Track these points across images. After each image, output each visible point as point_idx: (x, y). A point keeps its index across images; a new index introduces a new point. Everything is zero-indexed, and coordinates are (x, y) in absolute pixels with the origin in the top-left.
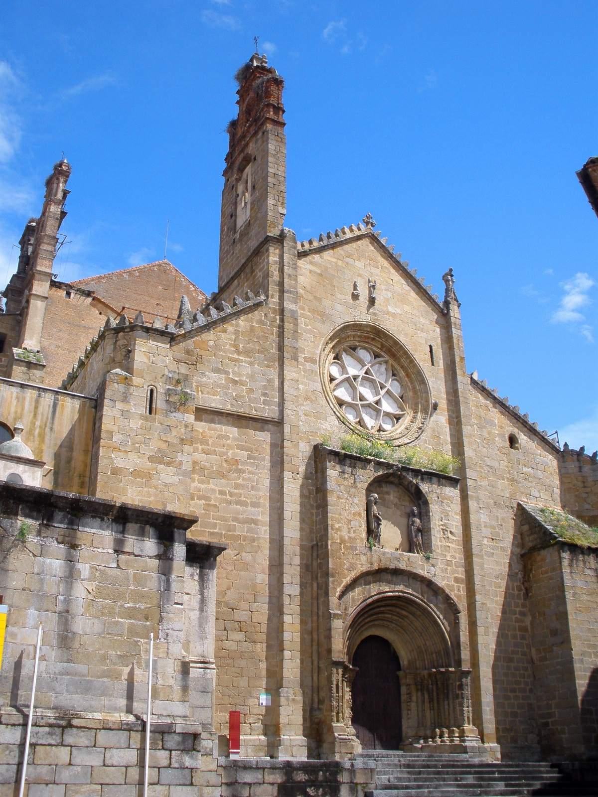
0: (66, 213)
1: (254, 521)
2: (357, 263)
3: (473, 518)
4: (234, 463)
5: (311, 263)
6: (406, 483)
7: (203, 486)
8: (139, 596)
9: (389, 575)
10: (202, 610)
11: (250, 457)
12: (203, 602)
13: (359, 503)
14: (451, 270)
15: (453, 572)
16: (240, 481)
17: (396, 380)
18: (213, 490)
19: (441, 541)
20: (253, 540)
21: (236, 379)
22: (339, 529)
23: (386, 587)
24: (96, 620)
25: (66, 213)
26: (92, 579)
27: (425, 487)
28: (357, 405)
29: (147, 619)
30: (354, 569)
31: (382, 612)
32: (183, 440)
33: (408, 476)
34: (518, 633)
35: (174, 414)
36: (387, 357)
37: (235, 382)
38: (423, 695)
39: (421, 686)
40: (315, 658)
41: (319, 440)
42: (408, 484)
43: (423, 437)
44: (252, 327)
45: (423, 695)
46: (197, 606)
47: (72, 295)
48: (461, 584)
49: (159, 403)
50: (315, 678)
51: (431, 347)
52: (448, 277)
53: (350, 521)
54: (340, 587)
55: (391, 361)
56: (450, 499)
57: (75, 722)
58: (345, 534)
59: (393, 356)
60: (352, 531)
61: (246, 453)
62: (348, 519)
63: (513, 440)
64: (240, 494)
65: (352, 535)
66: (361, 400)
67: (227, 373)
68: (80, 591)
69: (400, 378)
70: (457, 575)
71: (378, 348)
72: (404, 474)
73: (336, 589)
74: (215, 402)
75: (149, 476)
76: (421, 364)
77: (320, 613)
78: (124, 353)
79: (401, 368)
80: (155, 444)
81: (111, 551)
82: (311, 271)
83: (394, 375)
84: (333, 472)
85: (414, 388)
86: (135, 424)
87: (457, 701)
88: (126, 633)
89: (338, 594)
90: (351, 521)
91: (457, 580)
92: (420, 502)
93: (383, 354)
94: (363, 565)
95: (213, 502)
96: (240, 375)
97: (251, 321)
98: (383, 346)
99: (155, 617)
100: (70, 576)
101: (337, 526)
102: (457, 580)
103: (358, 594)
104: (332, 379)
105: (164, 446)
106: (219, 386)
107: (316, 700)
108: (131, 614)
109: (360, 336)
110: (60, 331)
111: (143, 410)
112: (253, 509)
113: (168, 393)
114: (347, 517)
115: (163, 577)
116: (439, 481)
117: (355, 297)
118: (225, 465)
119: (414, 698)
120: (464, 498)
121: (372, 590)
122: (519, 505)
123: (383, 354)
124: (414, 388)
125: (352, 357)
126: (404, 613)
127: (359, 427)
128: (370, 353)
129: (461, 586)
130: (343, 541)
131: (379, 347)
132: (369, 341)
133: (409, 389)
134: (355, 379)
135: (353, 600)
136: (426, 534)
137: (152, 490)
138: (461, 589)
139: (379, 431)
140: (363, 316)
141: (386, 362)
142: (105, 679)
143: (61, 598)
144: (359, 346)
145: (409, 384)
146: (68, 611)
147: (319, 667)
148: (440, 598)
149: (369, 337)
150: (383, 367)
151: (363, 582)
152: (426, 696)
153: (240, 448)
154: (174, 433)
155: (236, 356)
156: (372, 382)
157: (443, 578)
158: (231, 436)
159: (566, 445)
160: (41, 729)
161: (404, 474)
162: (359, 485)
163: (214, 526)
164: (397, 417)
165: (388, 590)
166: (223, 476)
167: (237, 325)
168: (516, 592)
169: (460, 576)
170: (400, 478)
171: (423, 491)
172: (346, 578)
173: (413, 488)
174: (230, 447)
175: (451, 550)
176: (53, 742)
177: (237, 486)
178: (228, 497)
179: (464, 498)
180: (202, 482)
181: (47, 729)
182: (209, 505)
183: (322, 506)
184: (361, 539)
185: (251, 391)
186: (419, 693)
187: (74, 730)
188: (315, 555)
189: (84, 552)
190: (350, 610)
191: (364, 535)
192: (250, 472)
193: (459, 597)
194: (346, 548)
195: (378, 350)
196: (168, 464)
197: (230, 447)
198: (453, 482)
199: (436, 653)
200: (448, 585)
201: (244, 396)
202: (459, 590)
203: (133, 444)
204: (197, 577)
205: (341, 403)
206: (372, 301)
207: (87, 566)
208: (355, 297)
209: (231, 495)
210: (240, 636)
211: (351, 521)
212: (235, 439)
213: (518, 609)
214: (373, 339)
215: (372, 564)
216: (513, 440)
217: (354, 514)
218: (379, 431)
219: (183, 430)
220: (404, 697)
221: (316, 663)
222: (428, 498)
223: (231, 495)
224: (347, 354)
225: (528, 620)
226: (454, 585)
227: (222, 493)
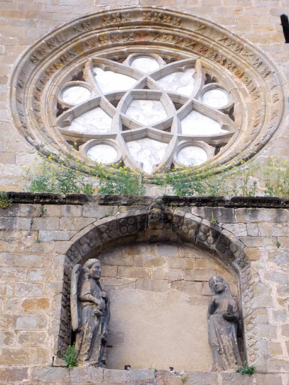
6: (192, 231)
13: (47, 279)
17: (217, 87)
27: (236, 229)
28: (114, 136)
33: (188, 216)
36: (190, 57)
42: (196, 233)
55: (200, 61)
60: (15, 339)
62: (7, 316)
65: (16, 346)
66: (124, 128)
69: (224, 82)
71: (171, 46)
72: (177, 211)
76: (258, 45)
79: (223, 65)
90: (15, 318)
109: (124, 35)
114: (7, 312)
123: (182, 53)
125: (116, 72)
128: (157, 60)
131: (173, 43)
132: (150, 39)
133: (245, 95)
136: (250, 326)
144: (130, 52)
145: (244, 86)
149: (146, 34)
150: (190, 73)
156: (159, 100)
161: (177, 211)
162: (49, 248)
164: (217, 142)
170: (167, 219)
171: (232, 238)
173: (210, 238)
184: (42, 353)
191: (51, 342)
205: (78, 141)
211: (15, 318)
214: (157, 34)
217: (27, 305)
222: (245, 250)
224: (106, 69)
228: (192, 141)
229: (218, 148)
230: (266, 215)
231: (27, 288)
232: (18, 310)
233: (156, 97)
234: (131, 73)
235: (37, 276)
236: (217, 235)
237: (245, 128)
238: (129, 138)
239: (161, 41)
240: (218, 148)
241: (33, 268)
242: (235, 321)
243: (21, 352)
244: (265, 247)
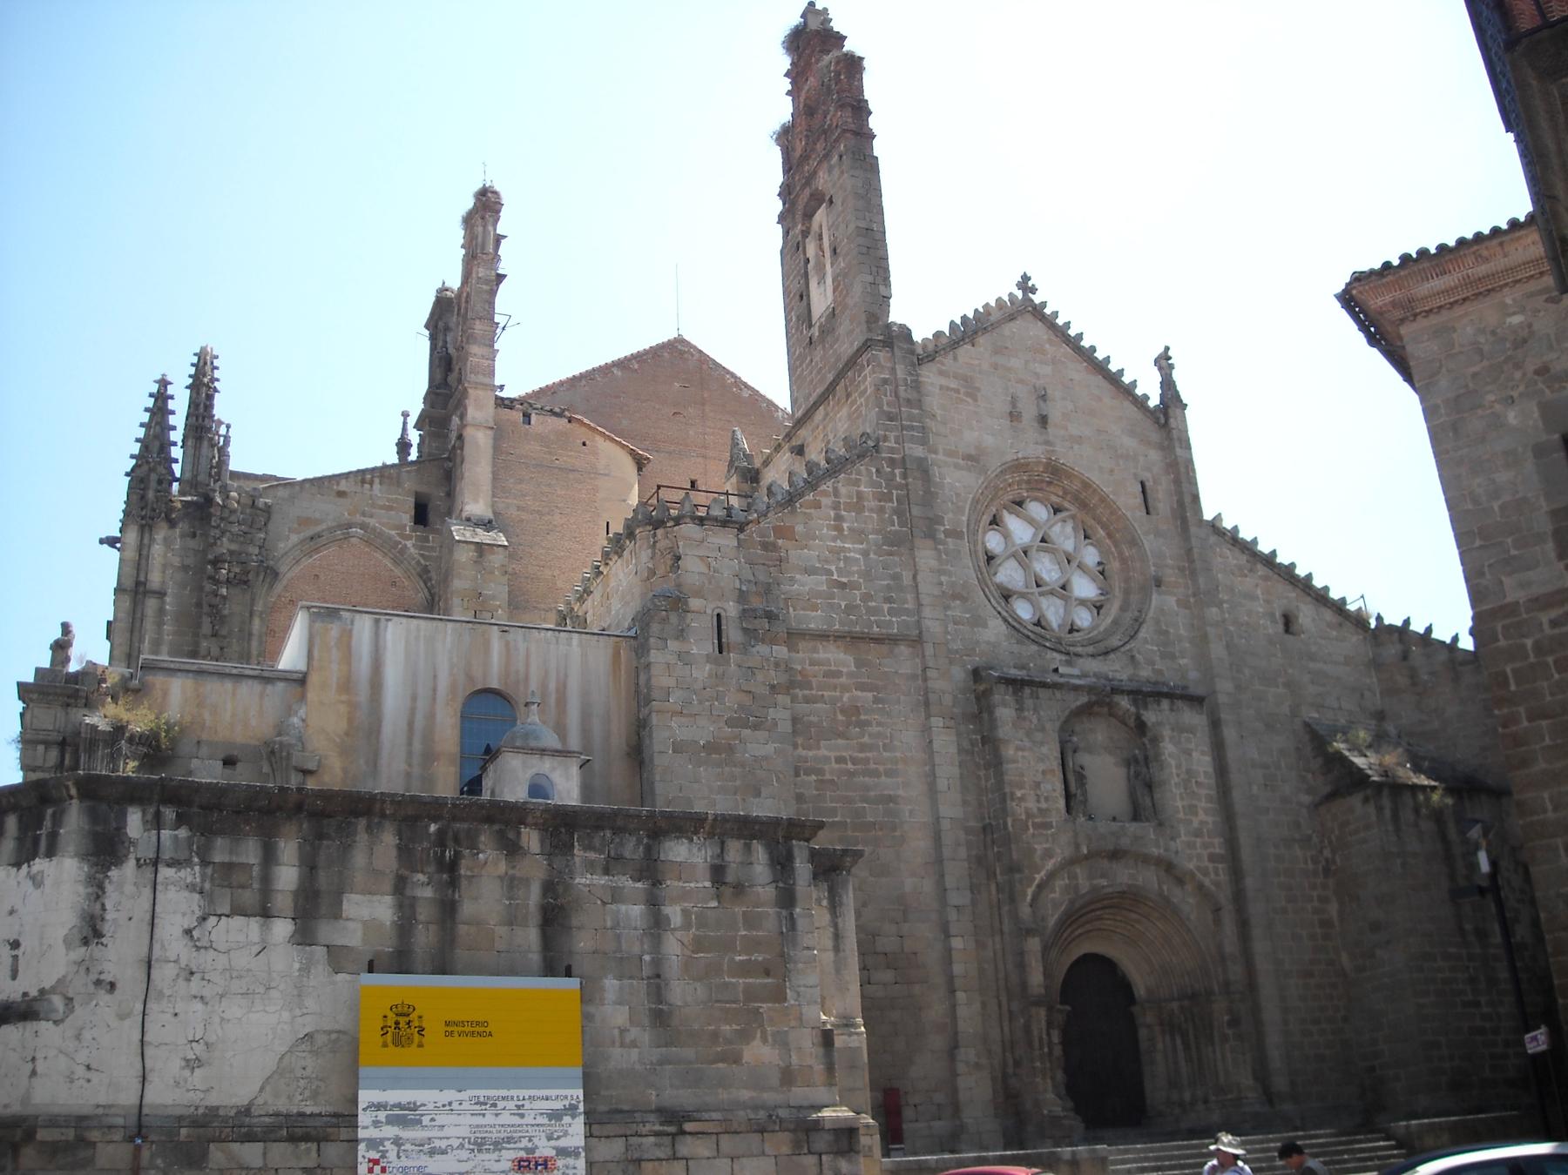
0: (504, 276)
1: (891, 799)
2: (1015, 363)
3: (1232, 754)
4: (853, 711)
5: (941, 373)
7: (811, 754)
8: (752, 945)
10: (837, 949)
11: (876, 700)
12: (837, 937)
13: (1051, 751)
14: (1167, 349)
15: (1205, 846)
16: (866, 739)
18: (827, 759)
19: (1182, 799)
20: (894, 829)
21: (844, 580)
22: (1022, 799)
24: (698, 985)
25: (504, 276)
26: (686, 926)
27: (1150, 717)
29: (767, 973)
30: (1051, 857)
31: (1100, 918)
32: (773, 687)
34: (1319, 931)
35: (757, 648)
36: (1073, 510)
37: (843, 586)
38: (1173, 1040)
40: (1004, 1000)
41: (977, 660)
43: (1142, 634)
44: (860, 496)
45: (1173, 1040)
46: (829, 944)
47: (534, 418)
49: (733, 634)
50: (1006, 1029)
51: (1143, 484)
52: (1164, 362)
53: (1038, 785)
54: (1029, 886)
56: (1191, 730)
57: (688, 1127)
58: (1031, 804)
59: (1083, 505)
61: (870, 695)
63: (1288, 622)
64: (867, 761)
65: (1044, 805)
66: (1038, 586)
67: (830, 573)
68: (673, 947)
74: (815, 620)
75: (730, 749)
76: (1129, 514)
77: (1006, 928)
78: (670, 563)
80: (732, 700)
81: (708, 884)
82: (941, 387)
83: (1086, 537)
84: (1005, 713)
85: (1121, 553)
86: (702, 673)
88: (741, 997)
89: (1029, 898)
91: (1212, 858)
92: (1146, 741)
93: (1066, 504)
94: (1062, 852)
95: (828, 777)
96: (850, 573)
97: (857, 483)
98: (1066, 492)
99: (776, 969)
100: (657, 923)
101: (1019, 794)
102: (1212, 858)
104: (990, 558)
105: (747, 700)
106: (819, 594)
107: (1011, 1062)
108: (745, 969)
109: (1028, 482)
110: (521, 481)
111: (710, 647)
112: (889, 780)
113: (745, 614)
115: (784, 913)
116: (1172, 703)
117: (1014, 416)
118: (840, 717)
119: (1160, 1046)
120: (1215, 725)
122: (1307, 725)
124: (1121, 553)
126: (1134, 916)
127: (1038, 629)
130: (1029, 815)
134: (1025, 553)
137: (737, 770)
139: (1071, 631)
140: (1030, 448)
141: (1073, 517)
142: (721, 1065)
143: (647, 958)
146: (658, 976)
147: (1010, 1012)
148: (1189, 887)
152: (1179, 1041)
153: (862, 687)
154: (760, 677)
155: (839, 543)
158: (845, 670)
159: (1379, 618)
160: (644, 1140)
163: (834, 812)
166: (841, 735)
167: (836, 493)
168: (1311, 866)
169: (1217, 851)
174: (845, 689)
175: (1201, 812)
176: (662, 1156)
177: (863, 748)
178: (850, 766)
179: (1215, 725)
180: (810, 749)
181: (652, 1139)
182: (822, 781)
183: (996, 763)
185: (867, 597)
186: (1168, 1038)
187: (689, 1138)
188: (989, 838)
189: (672, 884)
191: (1062, 803)
192: (879, 724)
193: (1217, 884)
194: (1035, 826)
195: (1058, 500)
196: (756, 727)
197: (845, 689)
198: (1196, 701)
200: (1198, 868)
201: (857, 606)
203: (700, 702)
204: (825, 903)
205: (1007, 596)
206: (1043, 420)
207: (678, 908)
208: (1014, 416)
209: (854, 761)
210: (888, 976)
212: (850, 675)
213: (1315, 894)
214: (1050, 483)
215: (1077, 846)
216: (1288, 622)
217: (1044, 773)
218: (1071, 631)
219: (772, 673)
220: (1144, 1045)
221: (1005, 1008)
223: (854, 761)
225: (1333, 909)
227: (840, 760)
228: (1083, 602)
229: (1099, 608)
230: (1165, 704)
231: (1042, 760)
232: (1039, 777)
233: (1052, 551)
234: (1031, 521)
235: (1044, 750)
236: (1138, 717)
237: (1117, 592)
238: (1041, 594)
239: (1052, 489)
240: (1099, 608)
241: (1042, 743)
242: (1150, 786)
243: (1047, 810)
244: (1167, 733)
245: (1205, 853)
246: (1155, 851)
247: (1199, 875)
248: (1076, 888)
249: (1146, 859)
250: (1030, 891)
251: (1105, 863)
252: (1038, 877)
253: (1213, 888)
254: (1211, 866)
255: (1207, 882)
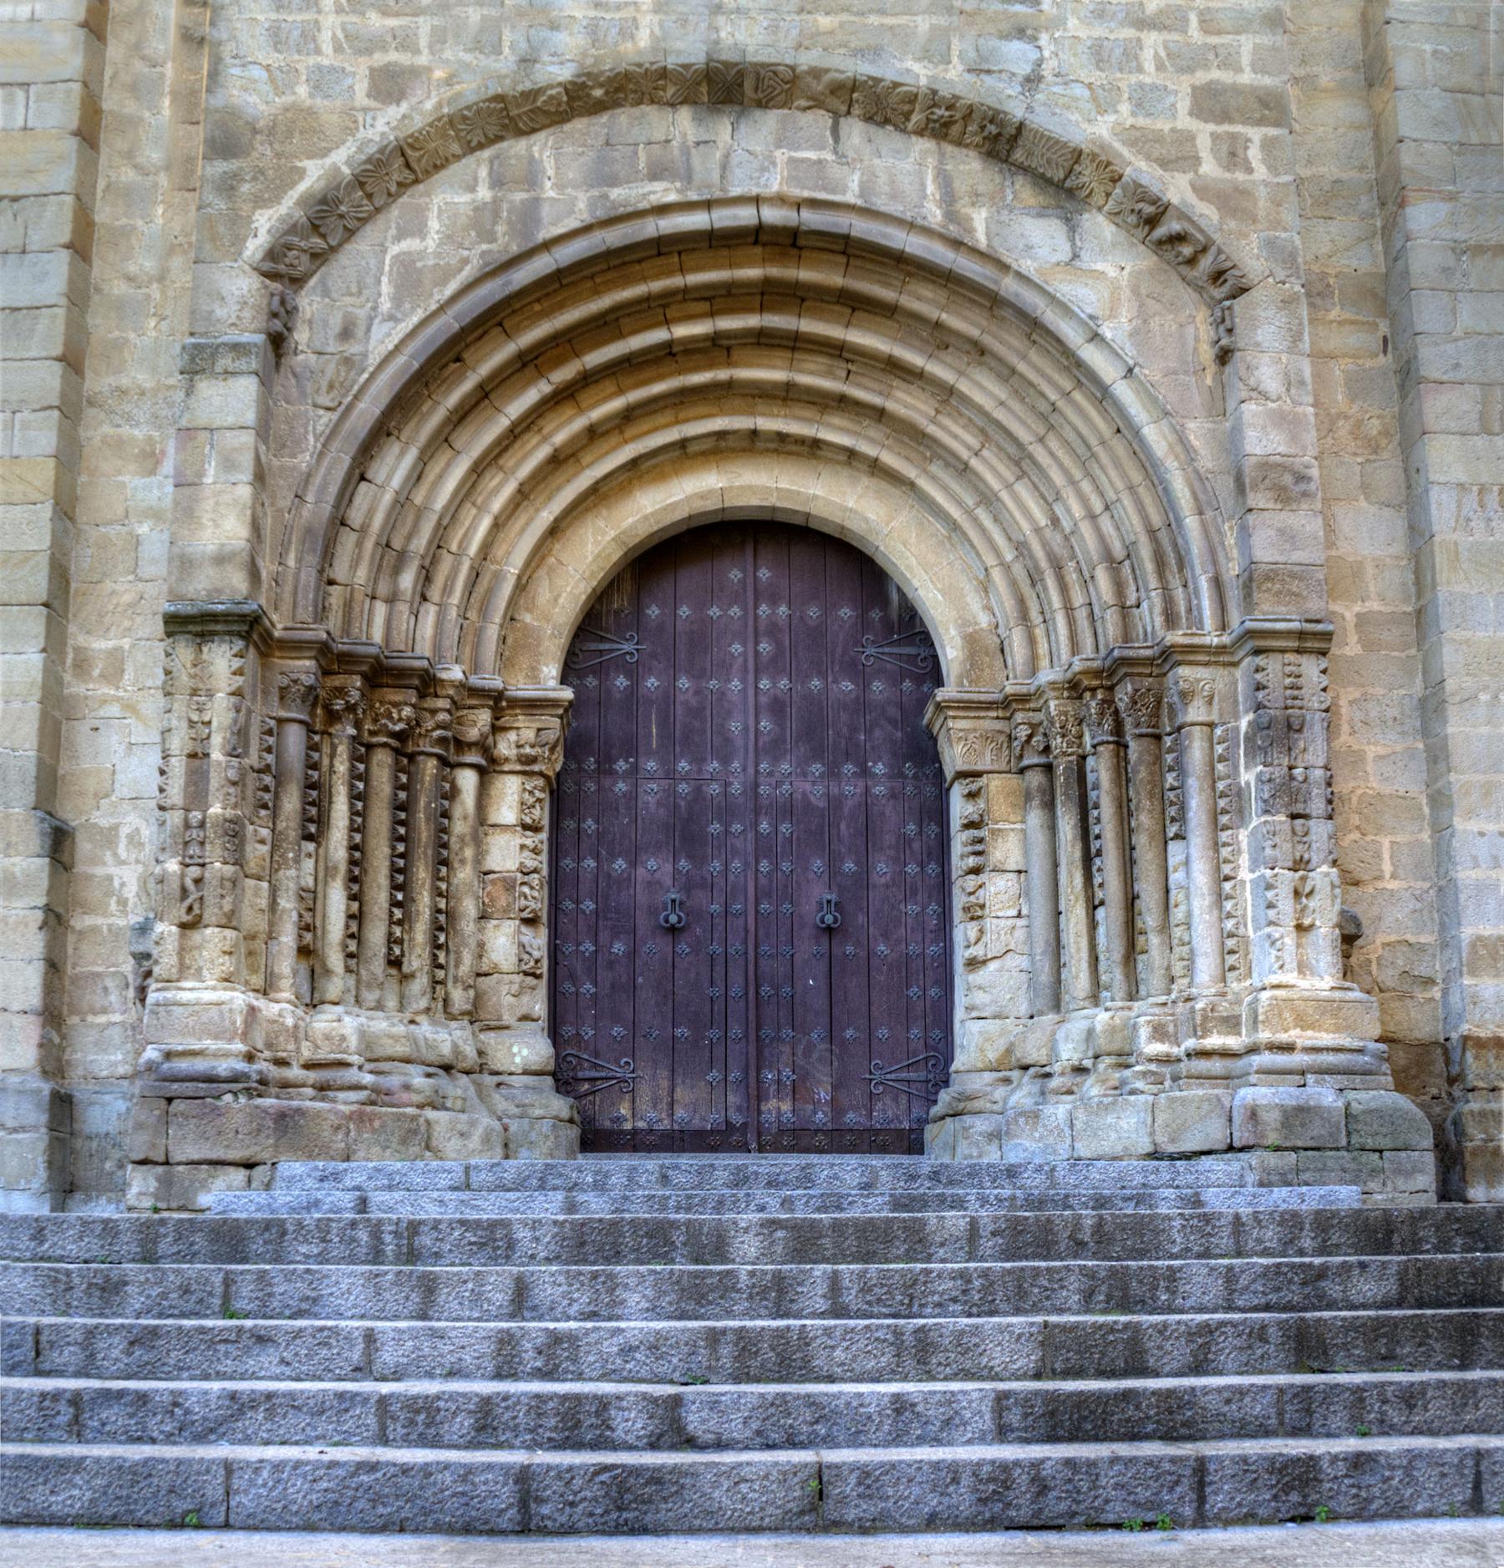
9: (684, 115)
23: (658, 186)
39: (1058, 784)
48: (1261, 122)
54: (276, 199)
70: (1216, 74)
73: (249, 220)
87: (1243, 835)
91: (1212, 103)
103: (448, 238)
121: (546, 212)
129: (1256, 134)
135: (409, 277)
138: (1254, 154)
151: (483, 172)
157: (1102, 102)
165: (672, 197)
169: (1247, 78)
172: (324, 153)
190: (382, 339)
193: (1232, 201)
199: (1114, 565)
200: (1139, 139)
202: (1233, 156)
226: (1190, 138)
245: (1183, 86)
246: (918, 73)
247: (1139, 168)
248: (529, 214)
249: (882, 106)
250: (265, 225)
251: (683, 124)
252: (314, 175)
253: (1207, 214)
254: (1204, 132)
255: (1176, 189)
